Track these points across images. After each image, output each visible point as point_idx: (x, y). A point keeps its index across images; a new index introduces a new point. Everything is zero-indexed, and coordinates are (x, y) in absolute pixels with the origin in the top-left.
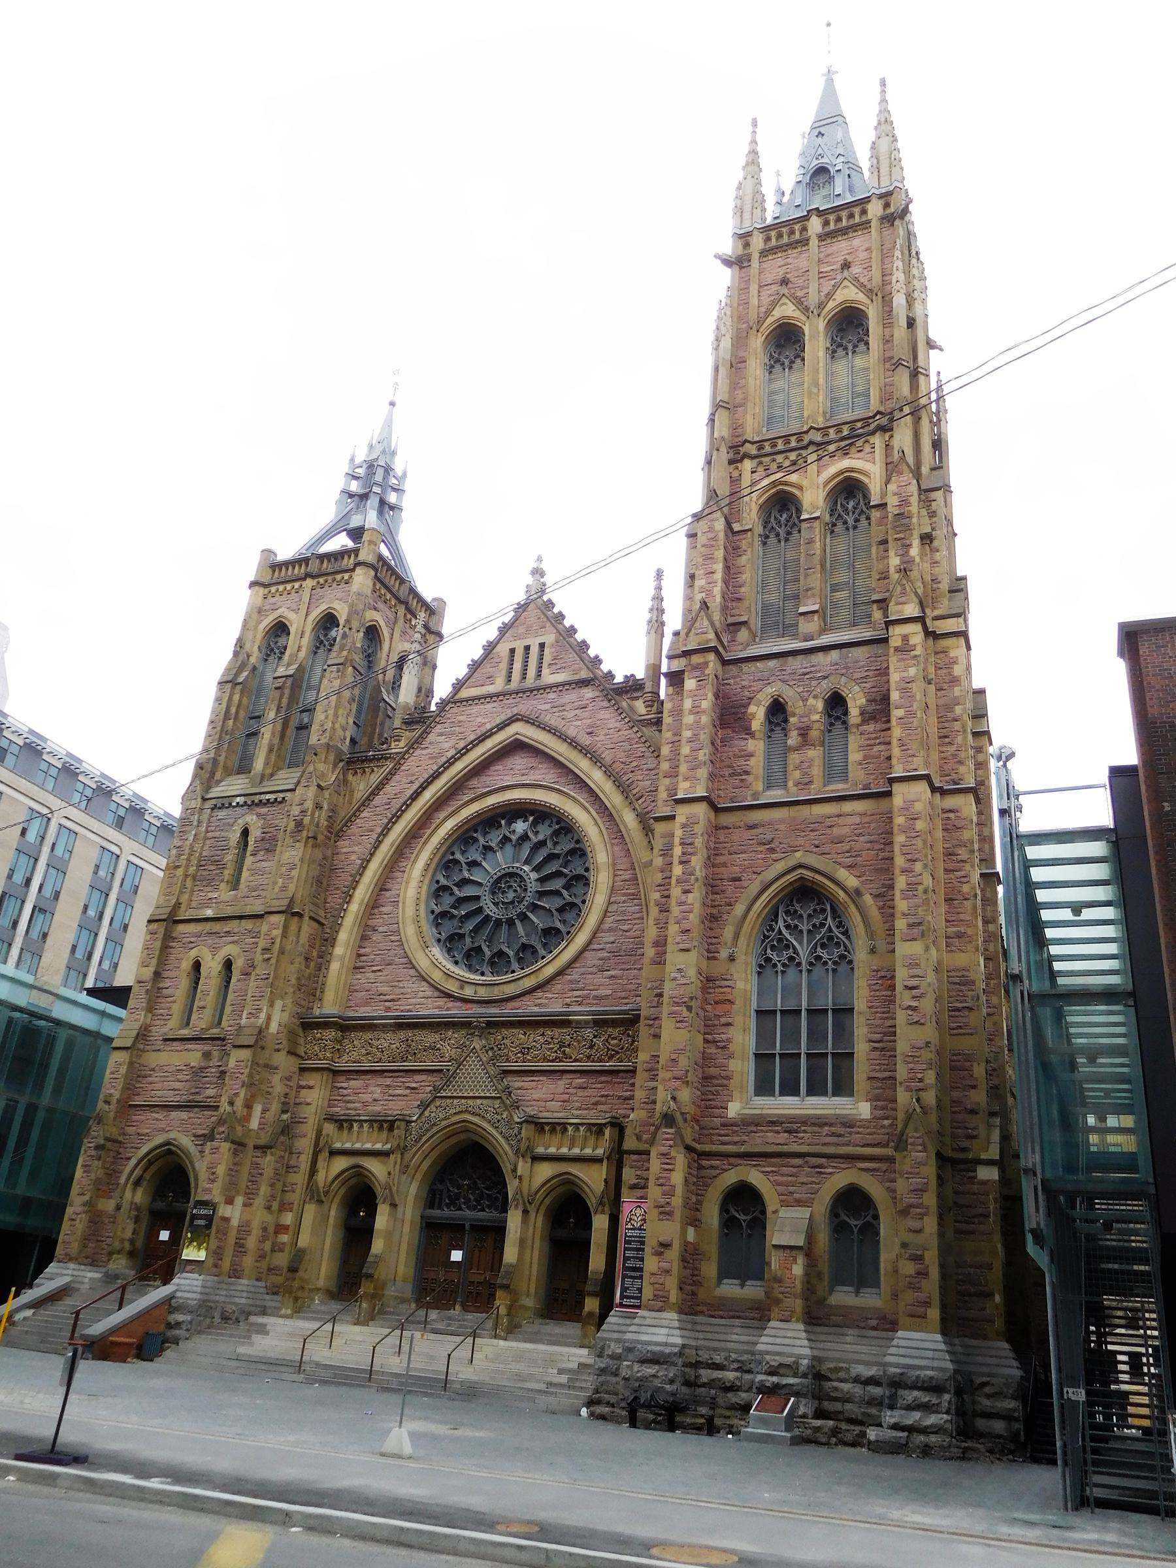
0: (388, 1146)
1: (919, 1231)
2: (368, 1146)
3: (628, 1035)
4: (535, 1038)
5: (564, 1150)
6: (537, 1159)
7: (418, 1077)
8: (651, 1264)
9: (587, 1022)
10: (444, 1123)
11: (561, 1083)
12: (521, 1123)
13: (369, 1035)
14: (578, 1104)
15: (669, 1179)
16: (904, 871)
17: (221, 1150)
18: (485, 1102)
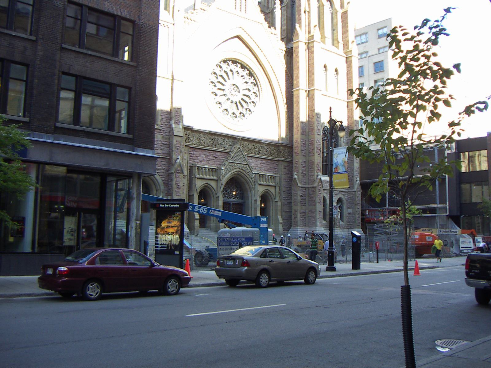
0: (215, 178)
1: (358, 208)
2: (208, 177)
3: (275, 150)
4: (250, 145)
5: (265, 183)
6: (260, 185)
7: (217, 153)
8: (318, 216)
9: (265, 143)
10: (232, 172)
11: (258, 161)
12: (255, 174)
13: (198, 135)
14: (264, 169)
15: (320, 196)
16: (356, 125)
17: (180, 177)
18: (244, 166)
